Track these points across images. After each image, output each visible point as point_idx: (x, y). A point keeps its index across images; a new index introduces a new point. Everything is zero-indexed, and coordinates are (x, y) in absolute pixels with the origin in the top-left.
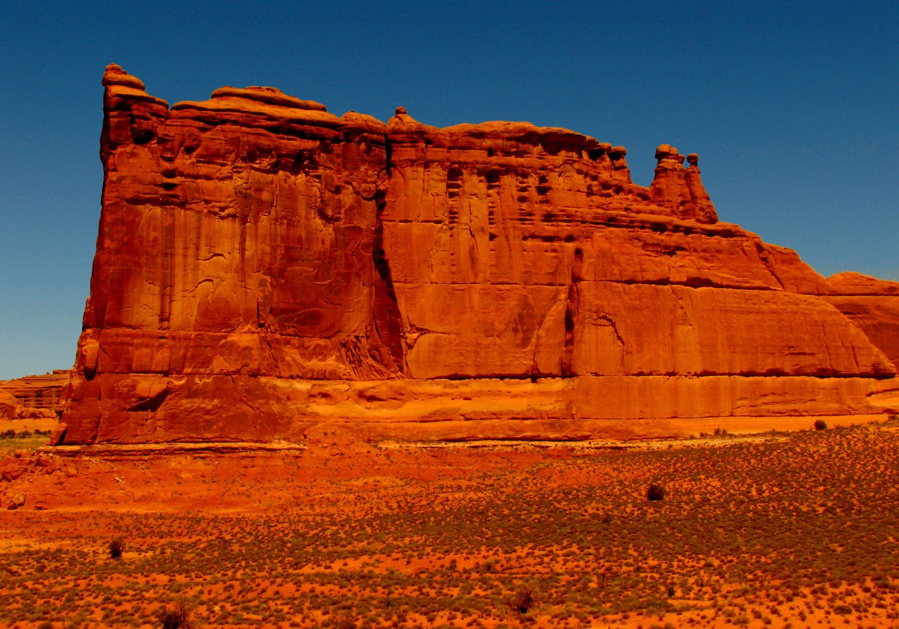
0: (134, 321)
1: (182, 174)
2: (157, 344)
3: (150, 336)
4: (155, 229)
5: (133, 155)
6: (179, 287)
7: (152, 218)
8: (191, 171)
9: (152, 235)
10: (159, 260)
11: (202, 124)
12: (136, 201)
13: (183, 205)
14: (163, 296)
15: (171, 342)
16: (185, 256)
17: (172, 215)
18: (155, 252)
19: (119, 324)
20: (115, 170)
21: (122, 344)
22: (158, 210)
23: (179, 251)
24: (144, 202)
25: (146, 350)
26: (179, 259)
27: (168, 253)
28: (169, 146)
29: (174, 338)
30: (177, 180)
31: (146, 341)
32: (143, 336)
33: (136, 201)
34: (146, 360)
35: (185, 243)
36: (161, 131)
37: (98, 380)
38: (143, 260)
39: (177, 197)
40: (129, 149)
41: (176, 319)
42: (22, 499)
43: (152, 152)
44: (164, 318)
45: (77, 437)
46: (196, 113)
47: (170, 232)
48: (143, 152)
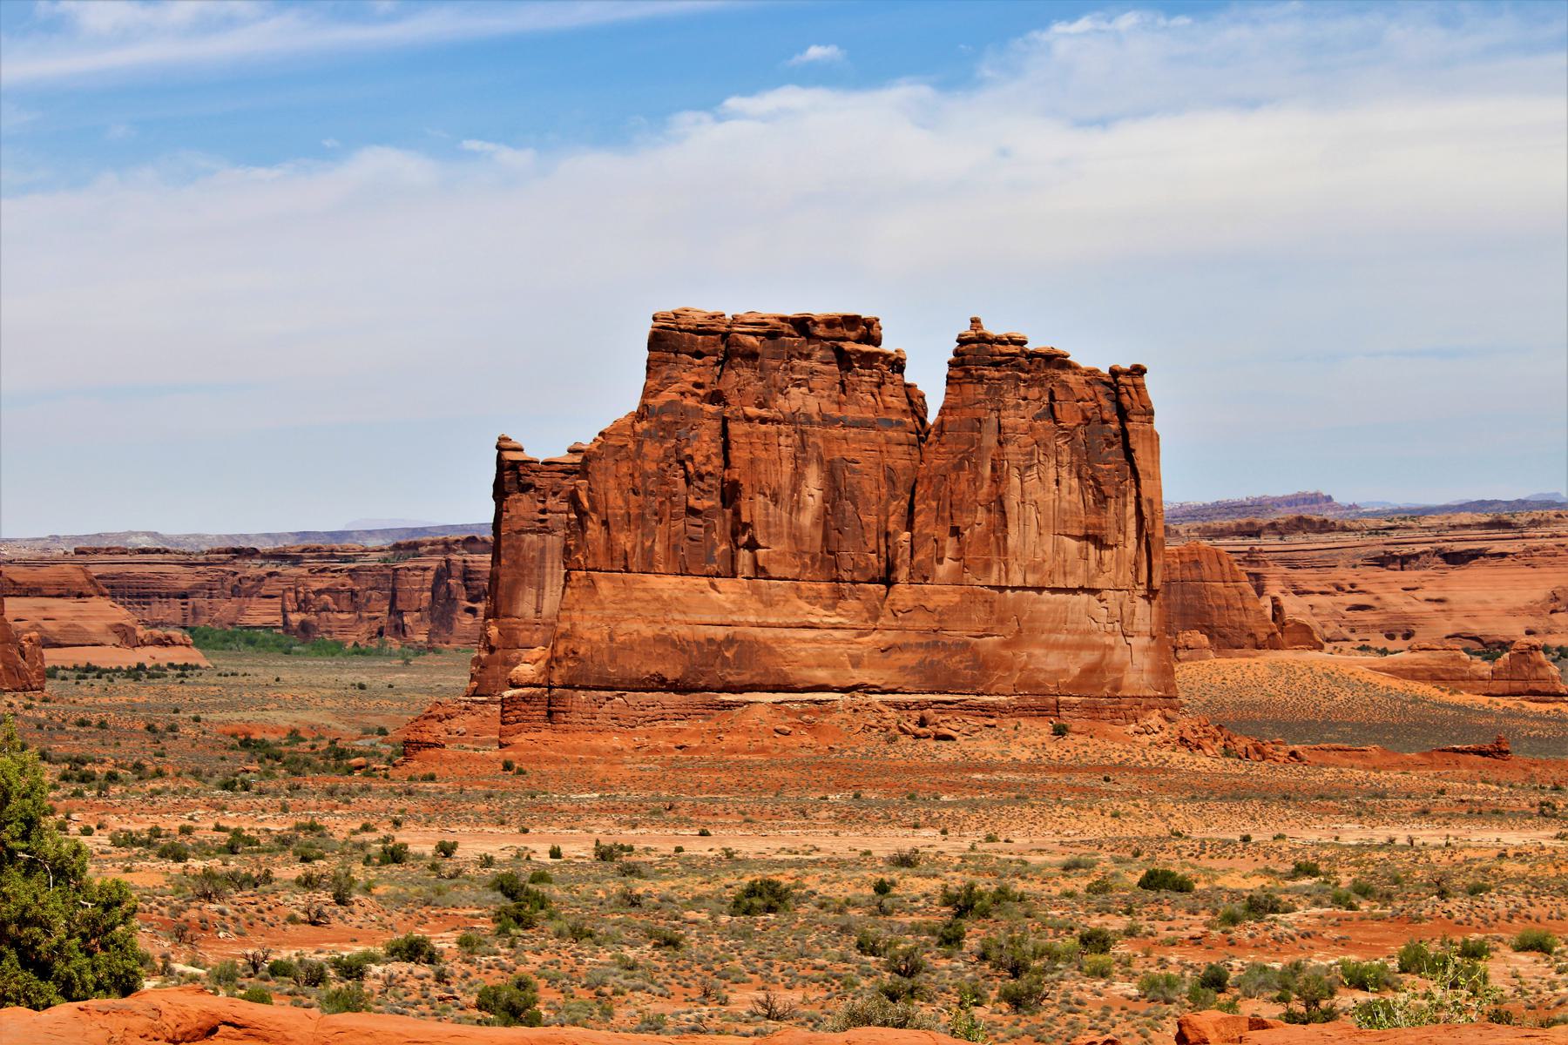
0: (519, 614)
1: (550, 512)
2: (534, 628)
3: (530, 624)
4: (533, 550)
5: (519, 500)
6: (548, 589)
7: (532, 542)
8: (555, 509)
9: (532, 554)
10: (536, 571)
11: (563, 475)
12: (521, 532)
13: (549, 533)
14: (538, 596)
15: (543, 627)
16: (552, 567)
17: (544, 540)
18: (533, 566)
19: (511, 616)
20: (508, 511)
21: (513, 629)
22: (535, 537)
23: (548, 565)
24: (527, 532)
25: (527, 633)
26: (548, 570)
27: (542, 567)
28: (542, 492)
29: (544, 624)
30: (548, 515)
31: (528, 627)
32: (525, 623)
33: (521, 532)
34: (527, 640)
35: (552, 557)
36: (538, 483)
37: (498, 653)
38: (525, 572)
39: (547, 528)
40: (516, 496)
41: (546, 611)
42: (464, 730)
43: (531, 497)
44: (538, 611)
45: (485, 692)
46: (560, 467)
47: (543, 551)
48: (525, 497)
